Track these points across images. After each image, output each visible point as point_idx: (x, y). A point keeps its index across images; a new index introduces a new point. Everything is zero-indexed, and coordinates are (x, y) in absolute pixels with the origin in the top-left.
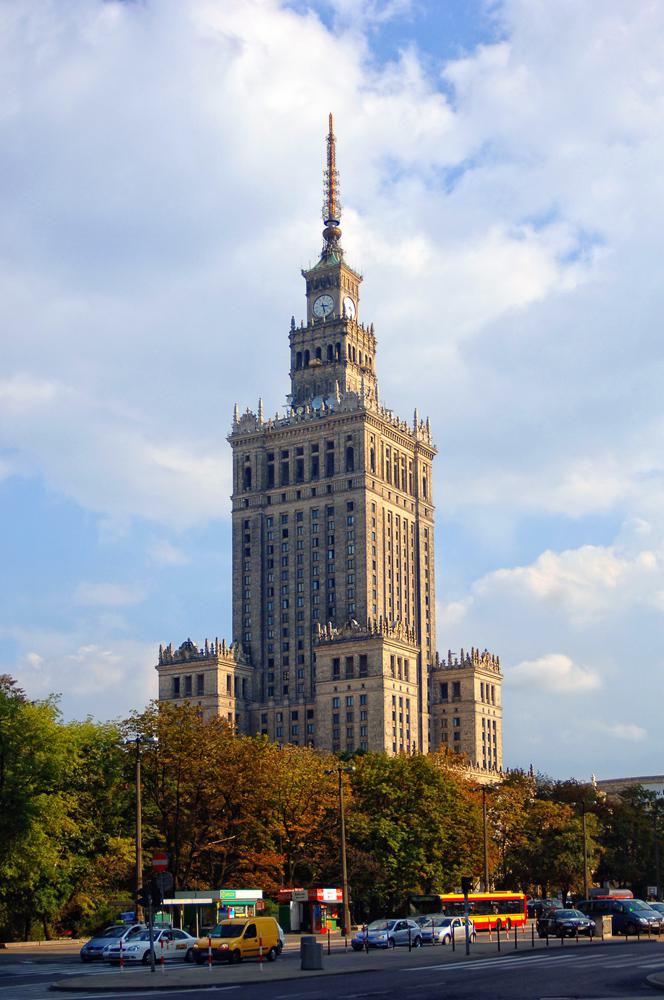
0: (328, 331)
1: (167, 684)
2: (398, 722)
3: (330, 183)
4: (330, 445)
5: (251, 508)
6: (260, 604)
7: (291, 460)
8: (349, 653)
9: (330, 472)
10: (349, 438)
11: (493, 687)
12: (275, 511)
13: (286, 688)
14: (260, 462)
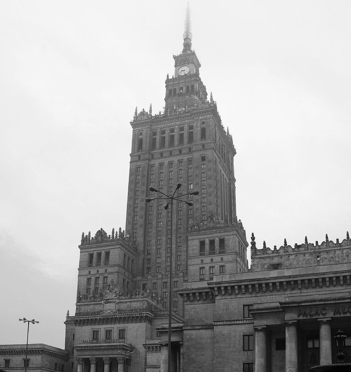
4: (191, 127)
5: (142, 160)
10: (203, 123)
12: (156, 162)
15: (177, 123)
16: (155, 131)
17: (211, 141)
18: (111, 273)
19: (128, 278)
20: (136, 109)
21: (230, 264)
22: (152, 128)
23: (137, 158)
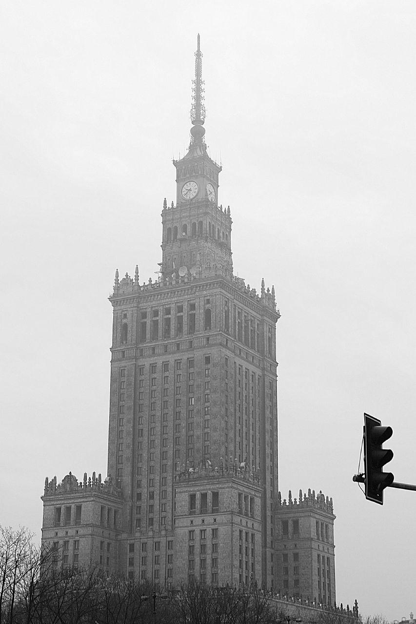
1: (50, 513)
2: (244, 555)
4: (193, 307)
8: (204, 490)
9: (192, 329)
11: (327, 526)
12: (146, 362)
13: (151, 520)
15: (173, 299)
16: (144, 310)
17: (218, 333)
18: (84, 536)
19: (109, 538)
20: (117, 273)
21: (224, 527)
22: (140, 306)
23: (120, 356)
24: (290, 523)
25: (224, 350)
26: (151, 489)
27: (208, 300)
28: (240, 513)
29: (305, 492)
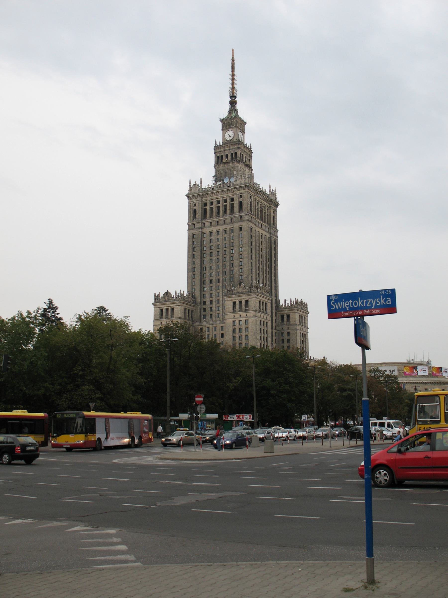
0: (232, 147)
3: (233, 79)
4: (232, 200)
6: (200, 274)
7: (214, 206)
12: (207, 230)
13: (211, 315)
14: (200, 207)
20: (190, 181)
24: (285, 316)
25: (250, 223)
26: (211, 299)
27: (241, 196)
28: (260, 311)
29: (293, 300)
